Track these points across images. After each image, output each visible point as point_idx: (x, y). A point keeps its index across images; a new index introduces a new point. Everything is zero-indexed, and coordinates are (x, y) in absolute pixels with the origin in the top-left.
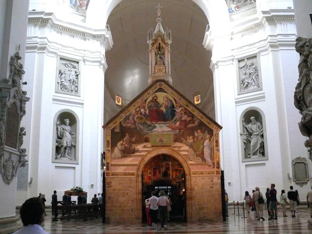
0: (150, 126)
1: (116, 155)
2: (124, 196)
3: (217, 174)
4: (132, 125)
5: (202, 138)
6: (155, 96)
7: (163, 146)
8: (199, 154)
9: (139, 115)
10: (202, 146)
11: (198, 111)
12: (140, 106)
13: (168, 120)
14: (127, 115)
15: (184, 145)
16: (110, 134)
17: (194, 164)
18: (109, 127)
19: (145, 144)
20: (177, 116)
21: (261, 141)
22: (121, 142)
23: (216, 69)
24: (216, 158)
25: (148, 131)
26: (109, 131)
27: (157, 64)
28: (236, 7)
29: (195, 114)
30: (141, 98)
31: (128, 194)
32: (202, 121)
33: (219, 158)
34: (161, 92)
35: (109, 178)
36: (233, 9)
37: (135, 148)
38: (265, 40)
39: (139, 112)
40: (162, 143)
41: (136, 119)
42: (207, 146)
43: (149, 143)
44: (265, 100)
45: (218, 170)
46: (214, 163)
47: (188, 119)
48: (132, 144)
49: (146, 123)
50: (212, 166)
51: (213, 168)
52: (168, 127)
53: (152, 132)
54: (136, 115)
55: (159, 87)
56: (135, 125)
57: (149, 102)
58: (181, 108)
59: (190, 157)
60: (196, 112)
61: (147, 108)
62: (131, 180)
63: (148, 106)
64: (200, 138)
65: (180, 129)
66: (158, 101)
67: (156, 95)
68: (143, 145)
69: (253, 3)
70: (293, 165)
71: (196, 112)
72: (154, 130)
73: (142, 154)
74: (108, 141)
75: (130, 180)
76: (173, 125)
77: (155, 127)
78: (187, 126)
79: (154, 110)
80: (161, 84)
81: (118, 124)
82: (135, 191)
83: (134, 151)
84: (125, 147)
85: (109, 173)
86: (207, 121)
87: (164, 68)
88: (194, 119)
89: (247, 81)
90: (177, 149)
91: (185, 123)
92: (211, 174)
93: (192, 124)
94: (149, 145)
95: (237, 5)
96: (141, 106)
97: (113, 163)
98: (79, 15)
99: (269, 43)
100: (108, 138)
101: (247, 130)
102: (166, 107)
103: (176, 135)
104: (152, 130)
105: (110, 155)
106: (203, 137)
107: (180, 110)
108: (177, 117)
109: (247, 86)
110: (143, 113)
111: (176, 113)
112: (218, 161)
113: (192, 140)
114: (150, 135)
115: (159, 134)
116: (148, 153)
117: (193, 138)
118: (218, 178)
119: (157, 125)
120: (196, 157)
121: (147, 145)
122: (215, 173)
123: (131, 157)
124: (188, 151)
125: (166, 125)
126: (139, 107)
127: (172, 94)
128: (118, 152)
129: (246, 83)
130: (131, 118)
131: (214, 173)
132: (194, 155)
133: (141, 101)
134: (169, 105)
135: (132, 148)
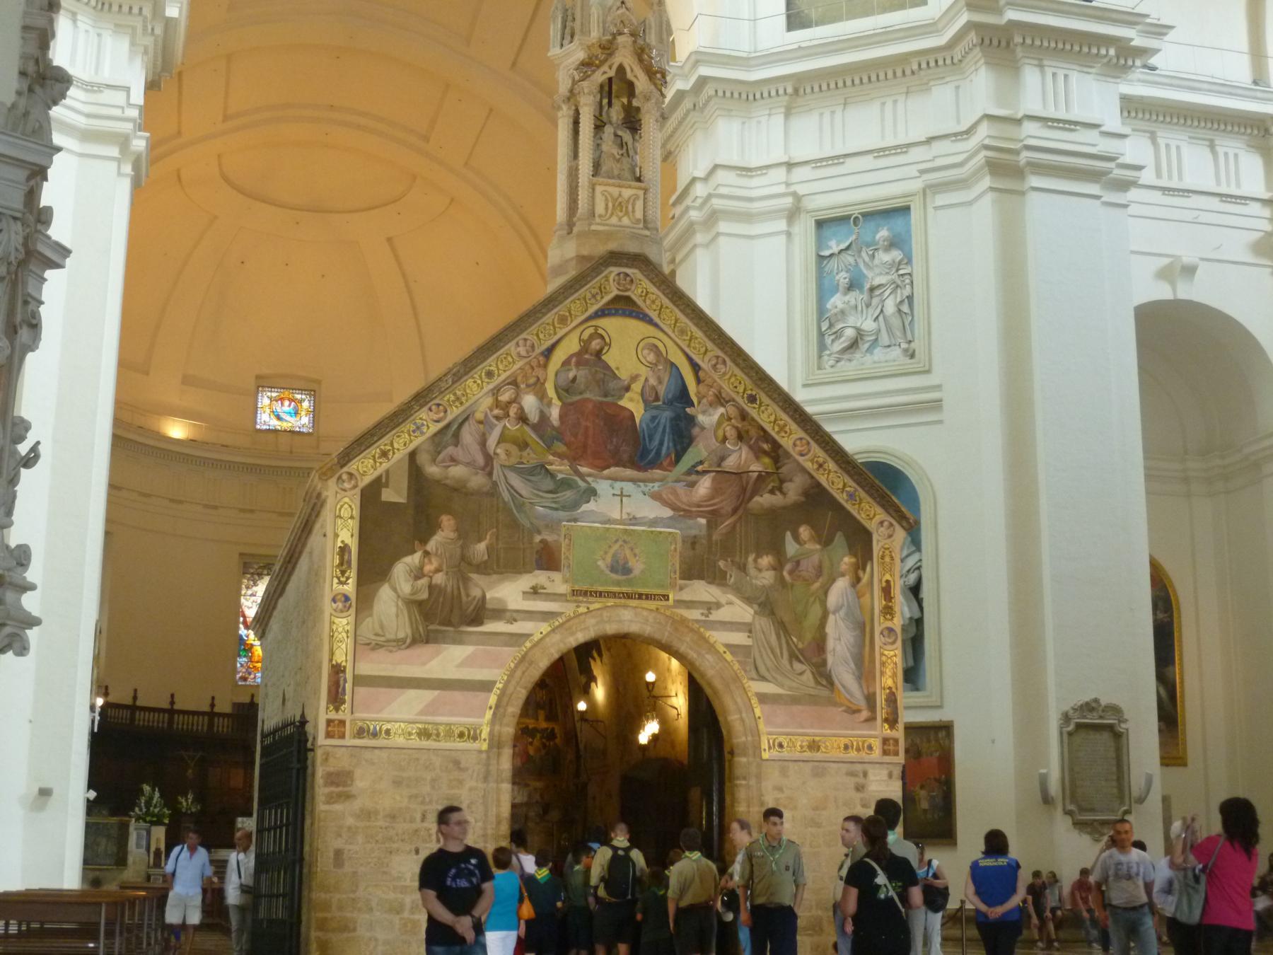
0: (566, 484)
1: (382, 627)
3: (885, 753)
4: (477, 474)
5: (819, 571)
7: (628, 596)
8: (800, 646)
9: (512, 427)
10: (816, 611)
11: (806, 431)
12: (519, 379)
13: (654, 464)
14: (450, 417)
15: (731, 597)
16: (356, 513)
17: (780, 696)
18: (351, 475)
19: (540, 577)
21: (908, 615)
22: (415, 558)
23: (699, 252)
24: (882, 673)
25: (556, 509)
26: (348, 493)
27: (604, 169)
29: (787, 442)
30: (525, 340)
32: (825, 484)
35: (340, 752)
37: (488, 596)
38: (955, 135)
39: (513, 411)
40: (624, 577)
41: (499, 443)
42: (842, 613)
43: (557, 576)
44: (940, 422)
45: (887, 732)
46: (871, 700)
47: (756, 467)
48: (474, 576)
49: (546, 469)
50: (865, 714)
51: (867, 720)
52: (656, 497)
53: (575, 520)
55: (615, 292)
56: (490, 474)
57: (566, 363)
58: (721, 410)
61: (551, 392)
62: (457, 763)
63: (562, 382)
64: (808, 566)
65: (714, 517)
66: (612, 365)
67: (600, 331)
68: (526, 582)
70: (1065, 737)
71: (794, 436)
72: (585, 507)
75: (451, 765)
76: (681, 488)
77: (592, 493)
79: (590, 406)
80: (627, 275)
81: (399, 461)
82: (480, 824)
83: (479, 613)
85: (342, 723)
86: (845, 485)
87: (637, 197)
88: (784, 470)
89: (858, 325)
90: (695, 614)
92: (858, 750)
93: (772, 492)
94: (556, 582)
96: (525, 376)
97: (366, 668)
99: (984, 153)
102: (650, 399)
103: (693, 544)
104: (575, 505)
105: (350, 628)
106: (826, 564)
107: (716, 417)
108: (700, 450)
109: (854, 345)
110: (534, 417)
111: (696, 431)
112: (890, 688)
114: (563, 531)
115: (608, 529)
117: (778, 567)
118: (890, 776)
119: (602, 486)
120: (785, 661)
123: (458, 641)
124: (748, 628)
125: (646, 490)
126: (514, 383)
127: (683, 332)
128: (394, 610)
129: (850, 333)
131: (870, 748)
132: (778, 651)
133: (522, 350)
134: (662, 390)
135: (468, 595)
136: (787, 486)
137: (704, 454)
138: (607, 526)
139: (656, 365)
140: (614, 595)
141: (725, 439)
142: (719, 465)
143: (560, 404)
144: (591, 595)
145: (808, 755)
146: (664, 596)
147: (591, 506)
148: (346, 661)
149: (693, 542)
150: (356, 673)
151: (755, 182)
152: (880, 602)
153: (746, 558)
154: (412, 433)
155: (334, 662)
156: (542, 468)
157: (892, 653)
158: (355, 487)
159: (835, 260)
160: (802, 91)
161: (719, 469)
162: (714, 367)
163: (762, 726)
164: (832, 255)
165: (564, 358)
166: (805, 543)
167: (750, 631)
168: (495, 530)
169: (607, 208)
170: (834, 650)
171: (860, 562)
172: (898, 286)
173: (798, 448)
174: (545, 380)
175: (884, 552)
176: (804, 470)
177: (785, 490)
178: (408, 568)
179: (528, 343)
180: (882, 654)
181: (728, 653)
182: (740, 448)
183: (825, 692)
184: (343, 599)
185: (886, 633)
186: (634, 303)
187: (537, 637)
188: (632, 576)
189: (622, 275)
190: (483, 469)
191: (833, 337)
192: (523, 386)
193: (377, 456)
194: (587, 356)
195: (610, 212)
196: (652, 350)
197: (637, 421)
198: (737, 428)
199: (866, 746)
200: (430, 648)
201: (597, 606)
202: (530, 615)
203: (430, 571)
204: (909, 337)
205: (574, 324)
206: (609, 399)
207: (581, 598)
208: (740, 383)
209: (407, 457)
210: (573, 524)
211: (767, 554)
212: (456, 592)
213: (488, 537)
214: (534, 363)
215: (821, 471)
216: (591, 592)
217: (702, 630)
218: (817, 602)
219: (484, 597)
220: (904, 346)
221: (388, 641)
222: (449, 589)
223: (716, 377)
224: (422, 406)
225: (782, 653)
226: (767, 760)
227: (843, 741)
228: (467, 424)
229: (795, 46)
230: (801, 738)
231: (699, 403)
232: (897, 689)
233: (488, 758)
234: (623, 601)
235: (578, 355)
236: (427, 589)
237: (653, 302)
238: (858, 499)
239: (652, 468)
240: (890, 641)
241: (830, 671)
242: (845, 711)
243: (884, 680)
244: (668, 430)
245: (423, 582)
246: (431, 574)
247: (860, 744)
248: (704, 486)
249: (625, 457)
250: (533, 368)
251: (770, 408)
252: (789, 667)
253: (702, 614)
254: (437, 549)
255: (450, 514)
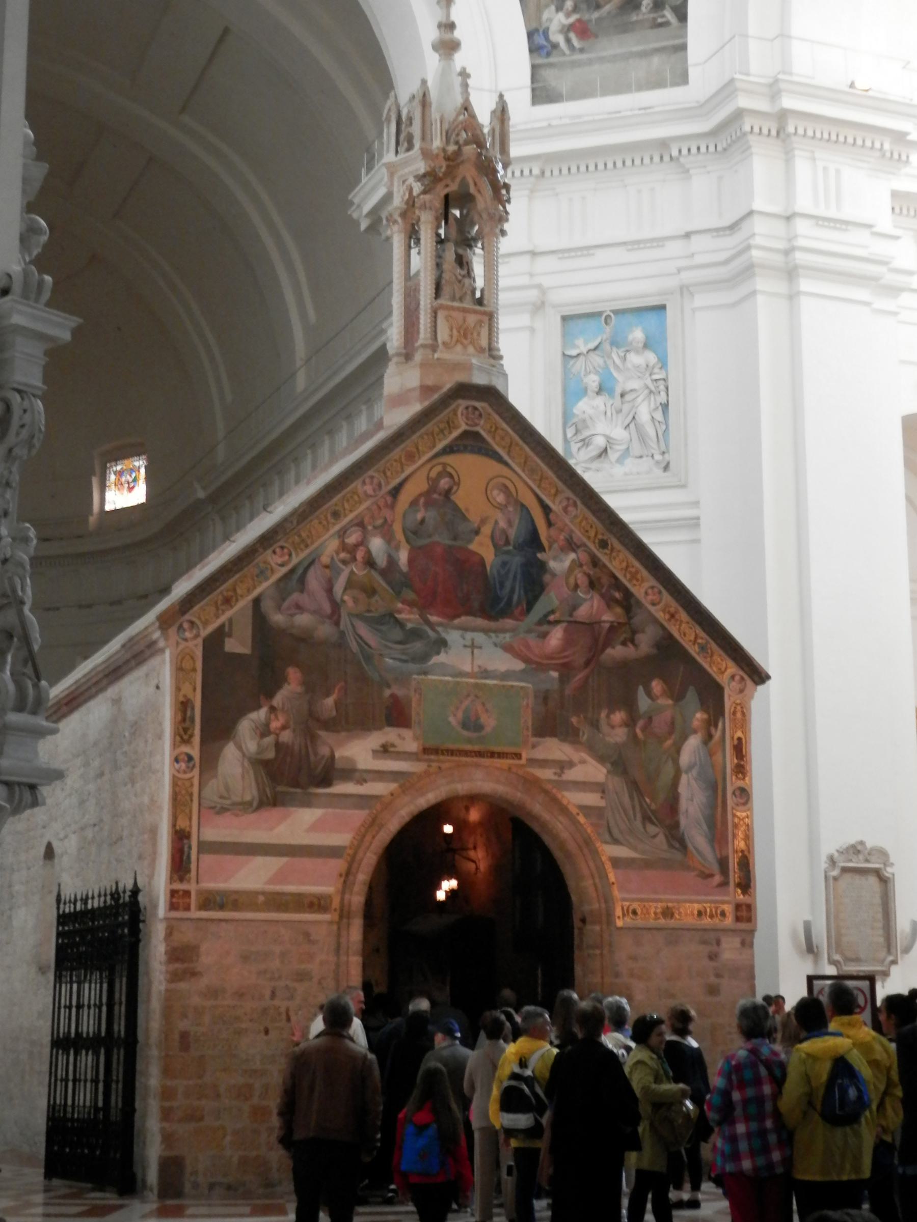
0: (416, 634)
1: (227, 789)
2: (267, 1032)
3: (738, 919)
6: (444, 473)
7: (479, 754)
8: (653, 807)
9: (359, 571)
10: (668, 770)
12: (366, 520)
13: (504, 613)
14: (295, 560)
15: (584, 755)
18: (192, 623)
19: (390, 735)
20: (553, 594)
22: (261, 714)
25: (405, 661)
28: (571, 27)
29: (638, 591)
30: (372, 477)
31: (293, 1018)
32: (676, 634)
33: (748, 838)
34: (472, 451)
36: (560, 39)
37: (337, 755)
39: (360, 555)
41: (345, 589)
42: (694, 772)
43: (407, 733)
46: (723, 864)
47: (608, 617)
48: (322, 733)
49: (396, 618)
50: (718, 879)
52: (508, 648)
53: (425, 673)
54: (341, 565)
55: (464, 427)
56: (337, 624)
57: (414, 503)
58: (572, 556)
59: (612, 824)
60: (646, 585)
61: (400, 536)
62: (307, 935)
64: (660, 723)
65: (566, 669)
66: (461, 505)
67: (449, 469)
68: (375, 740)
69: (666, 24)
70: (831, 881)
71: (646, 585)
76: (532, 640)
77: (442, 644)
78: (603, 650)
80: (475, 408)
84: (278, 745)
86: (696, 637)
89: (608, 433)
90: (547, 774)
92: (711, 916)
93: (624, 643)
95: (579, 21)
96: (373, 517)
97: (211, 834)
100: (187, 689)
102: (499, 542)
104: (424, 658)
107: (567, 563)
108: (551, 599)
110: (381, 561)
111: (547, 578)
112: (742, 851)
113: (625, 730)
114: (413, 683)
115: (458, 683)
116: (404, 789)
117: (630, 723)
119: (453, 637)
120: (638, 823)
121: (397, 741)
122: (728, 908)
124: (601, 789)
126: (361, 524)
128: (239, 770)
129: (600, 442)
130: (314, 581)
131: (723, 914)
132: (631, 813)
133: (369, 489)
134: (512, 533)
135: (316, 754)
136: (639, 637)
137: (556, 603)
138: (458, 679)
139: (506, 506)
140: (466, 753)
141: (576, 586)
142: (571, 615)
143: (408, 547)
144: (443, 754)
145: (662, 922)
146: (516, 754)
147: (441, 658)
148: (190, 826)
149: (544, 697)
150: (201, 839)
152: (732, 760)
153: (599, 714)
154: (255, 578)
155: (178, 828)
156: (390, 618)
157: (744, 814)
158: (197, 636)
159: (582, 358)
160: (548, 173)
161: (572, 619)
162: (565, 510)
163: (616, 893)
164: (579, 355)
165: (410, 499)
166: (658, 698)
167: (603, 792)
168: (342, 684)
169: (451, 336)
170: (687, 811)
171: (712, 718)
172: (651, 392)
173: (650, 597)
174: (393, 521)
175: (735, 708)
176: (656, 621)
177: (636, 642)
178: (253, 725)
179: (375, 481)
180: (734, 816)
181: (581, 814)
182: (592, 597)
183: (678, 856)
184: (186, 759)
185: (737, 793)
186: (483, 440)
188: (483, 733)
189: (470, 409)
190: (330, 617)
191: (580, 444)
192: (370, 528)
193: (219, 602)
194: (435, 496)
195: (454, 339)
196: (501, 490)
197: (488, 568)
198: (588, 576)
199: (719, 912)
200: (276, 812)
201: (447, 765)
203: (276, 728)
204: (663, 448)
205: (420, 462)
206: (458, 543)
207: (432, 757)
208: (591, 527)
209: (250, 605)
210: (423, 677)
211: (619, 710)
212: (303, 752)
213: (336, 691)
214: (381, 503)
215: (673, 621)
216: (442, 751)
217: (554, 791)
218: (670, 763)
219: (332, 757)
220: (658, 457)
221: (234, 804)
222: (296, 748)
223: (567, 521)
224: (265, 549)
225: (635, 816)
226: (621, 928)
227: (696, 907)
228: (312, 569)
229: (545, 124)
230: (655, 904)
231: (550, 547)
232: (749, 852)
233: (339, 929)
234: (475, 759)
235: (427, 494)
236: (274, 749)
237: (502, 438)
238: (709, 651)
239: (503, 617)
240: (742, 801)
241: (683, 834)
242: (698, 876)
243: (736, 842)
244: (519, 577)
245: (270, 740)
246: (278, 732)
247: (714, 910)
248: (556, 637)
249: (476, 605)
250: (379, 508)
251: (621, 556)
252: (642, 830)
253: (555, 774)
254: (283, 704)
255: (298, 666)
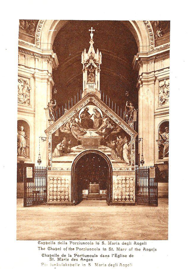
0: (82, 132)
14: (64, 122)
16: (51, 138)
19: (79, 146)
22: (60, 144)
39: (74, 121)
45: (133, 167)
47: (112, 127)
50: (129, 164)
52: (96, 133)
61: (80, 118)
68: (76, 147)
71: (118, 122)
73: (75, 153)
74: (49, 144)
80: (91, 98)
83: (70, 151)
91: (109, 130)
94: (80, 146)
98: (29, 36)
101: (162, 138)
110: (77, 122)
119: (88, 132)
120: (116, 157)
130: (67, 125)
145: (120, 171)
151: (149, 75)
187: (78, 155)
202: (77, 151)
235: (84, 111)
